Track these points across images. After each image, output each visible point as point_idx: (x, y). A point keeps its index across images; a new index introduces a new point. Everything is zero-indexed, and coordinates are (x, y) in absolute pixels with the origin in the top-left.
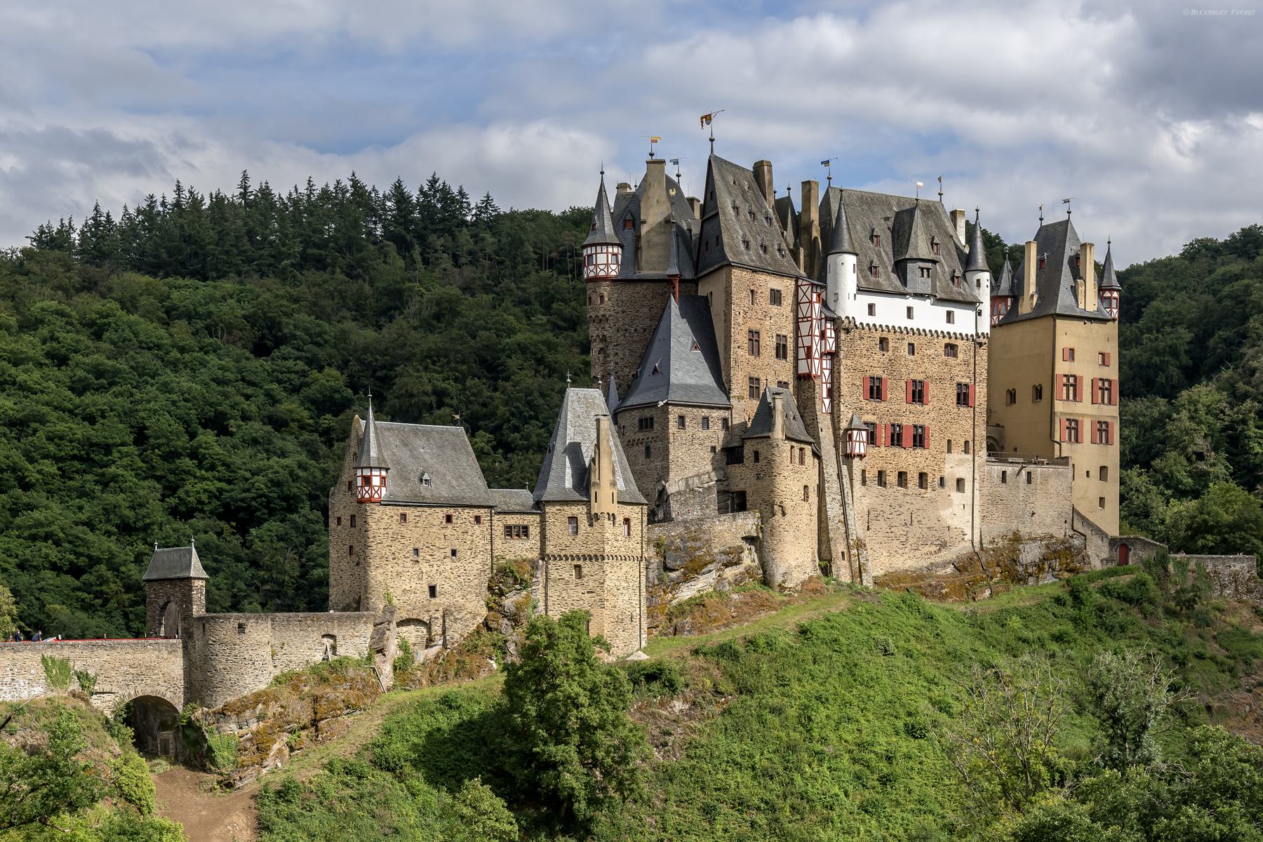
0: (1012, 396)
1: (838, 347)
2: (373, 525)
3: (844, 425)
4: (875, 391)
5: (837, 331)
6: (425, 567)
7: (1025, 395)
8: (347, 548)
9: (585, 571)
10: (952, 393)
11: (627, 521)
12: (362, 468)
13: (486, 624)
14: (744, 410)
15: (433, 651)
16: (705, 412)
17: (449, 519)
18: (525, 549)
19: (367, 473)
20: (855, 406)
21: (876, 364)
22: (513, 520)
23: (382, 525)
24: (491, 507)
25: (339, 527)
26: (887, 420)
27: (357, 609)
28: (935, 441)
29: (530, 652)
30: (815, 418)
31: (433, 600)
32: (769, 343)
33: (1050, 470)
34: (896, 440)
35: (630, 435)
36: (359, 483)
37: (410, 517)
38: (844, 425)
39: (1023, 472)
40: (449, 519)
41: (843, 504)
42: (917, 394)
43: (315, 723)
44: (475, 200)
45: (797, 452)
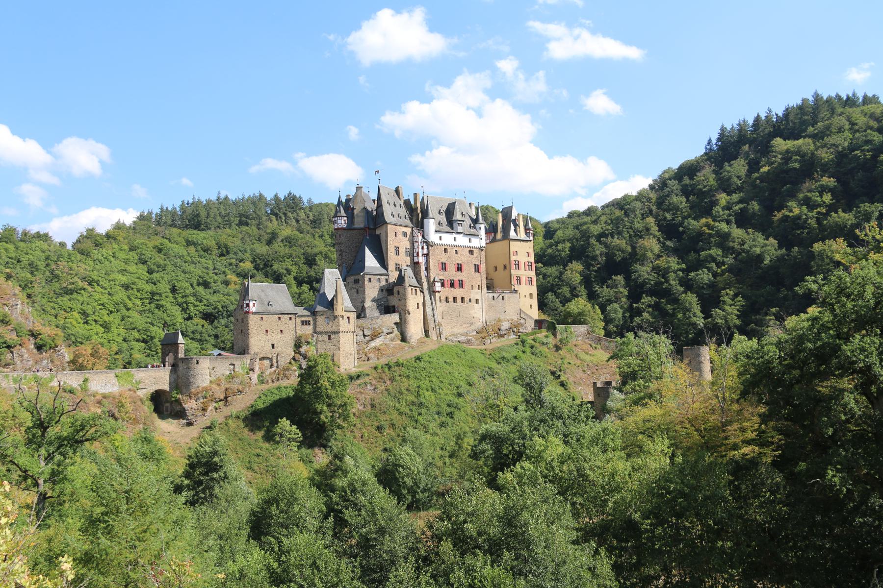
0: (496, 269)
2: (250, 322)
3: (432, 280)
4: (444, 267)
5: (428, 246)
6: (269, 336)
7: (500, 268)
10: (473, 267)
11: (348, 318)
13: (294, 359)
14: (393, 276)
15: (274, 369)
16: (379, 277)
17: (280, 318)
19: (248, 302)
20: (436, 273)
21: (443, 258)
22: (304, 319)
24: (295, 314)
26: (448, 278)
27: (244, 354)
28: (466, 284)
29: (310, 368)
30: (421, 278)
32: (402, 251)
33: (510, 295)
34: (452, 285)
35: (351, 286)
38: (432, 280)
39: (501, 296)
40: (280, 318)
41: (433, 310)
42: (459, 268)
43: (226, 398)
44: (305, 201)
45: (414, 291)
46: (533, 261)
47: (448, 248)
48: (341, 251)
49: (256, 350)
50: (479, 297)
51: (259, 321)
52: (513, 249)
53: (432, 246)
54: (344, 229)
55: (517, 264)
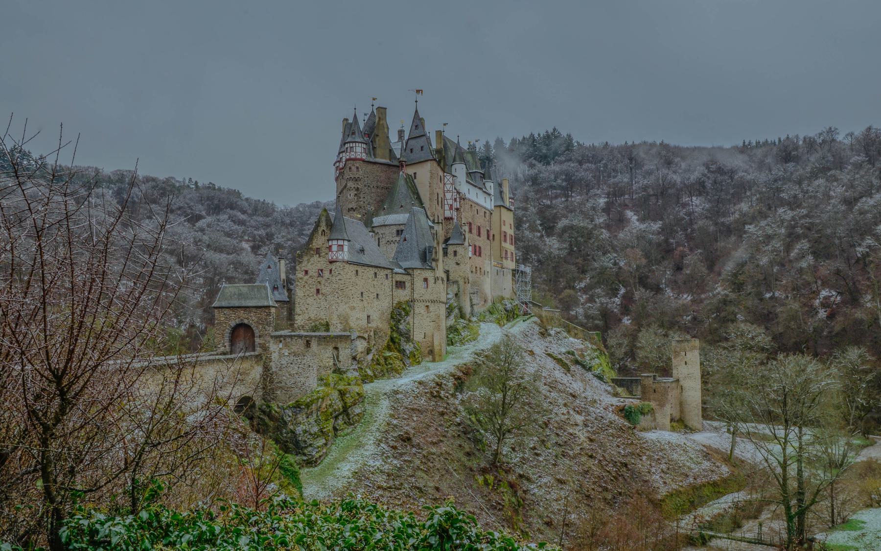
1: (461, 206)
5: (461, 198)
6: (365, 302)
8: (314, 290)
9: (431, 309)
10: (486, 232)
12: (338, 240)
13: (392, 339)
18: (403, 295)
22: (399, 278)
23: (348, 277)
24: (392, 269)
25: (306, 277)
31: (370, 325)
36: (335, 248)
37: (360, 273)
40: (376, 274)
46: (513, 234)
47: (473, 205)
48: (357, 189)
49: (352, 324)
50: (488, 269)
51: (354, 277)
52: (503, 218)
53: (464, 199)
54: (364, 161)
55: (505, 236)
